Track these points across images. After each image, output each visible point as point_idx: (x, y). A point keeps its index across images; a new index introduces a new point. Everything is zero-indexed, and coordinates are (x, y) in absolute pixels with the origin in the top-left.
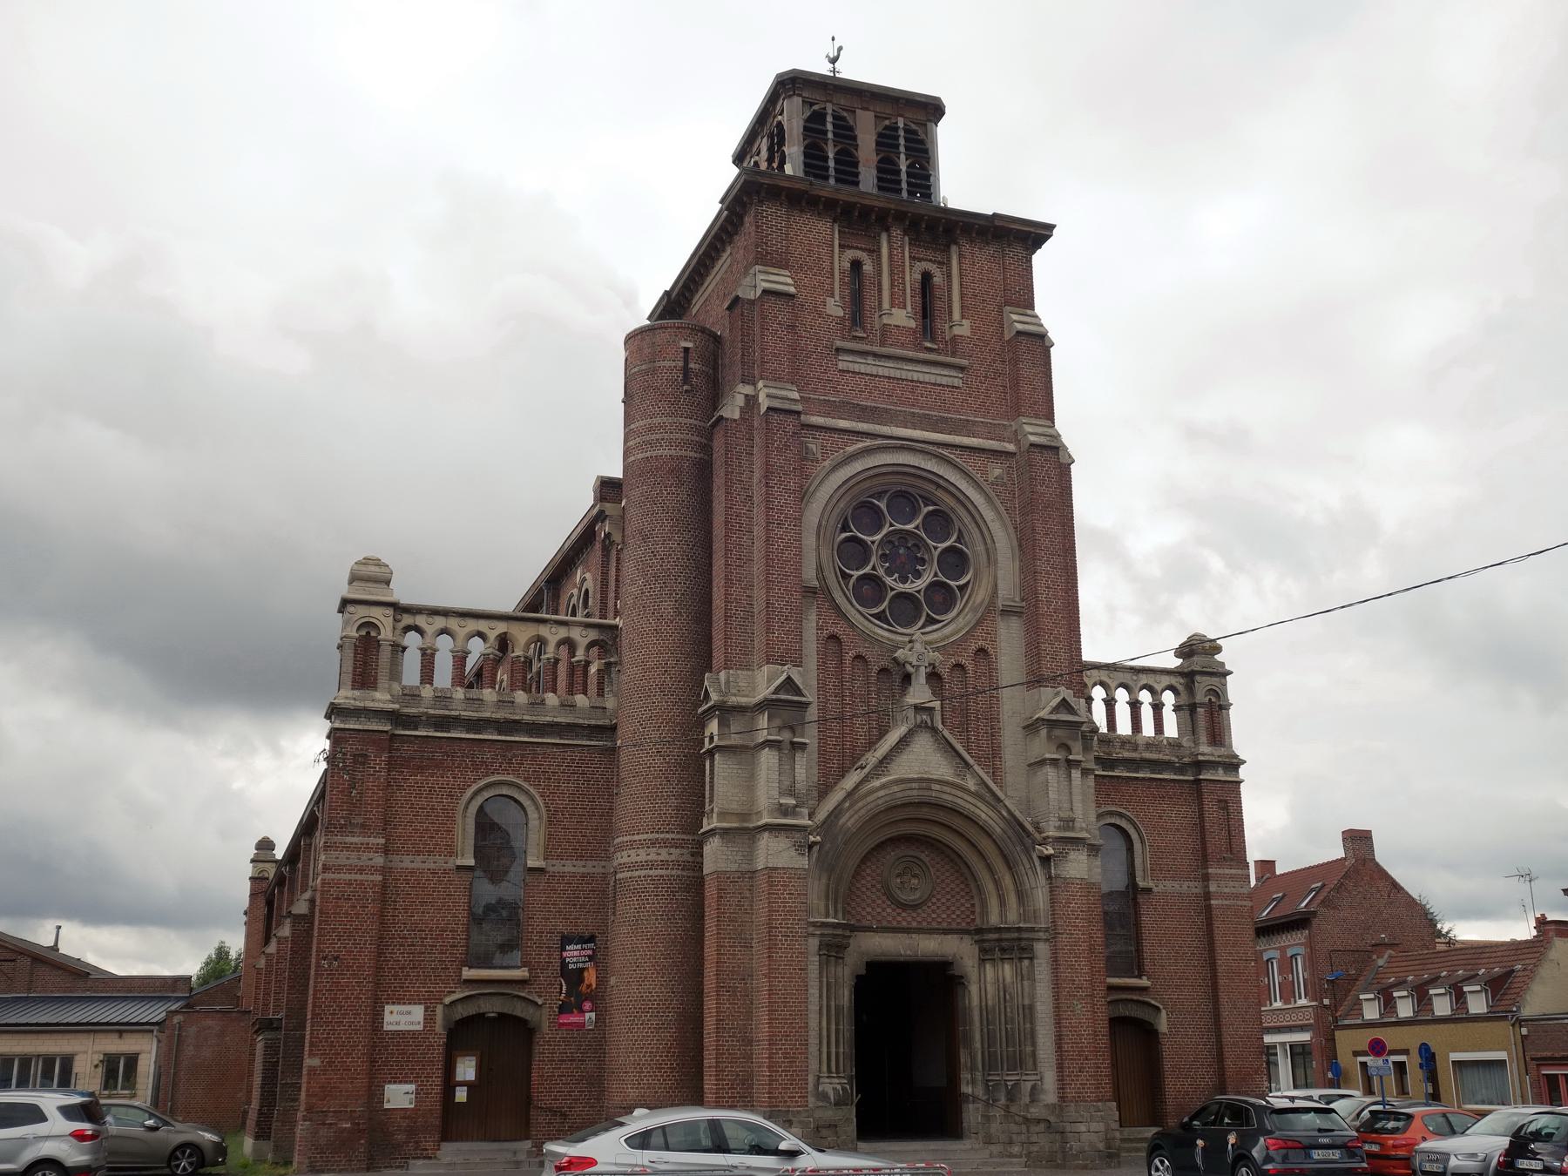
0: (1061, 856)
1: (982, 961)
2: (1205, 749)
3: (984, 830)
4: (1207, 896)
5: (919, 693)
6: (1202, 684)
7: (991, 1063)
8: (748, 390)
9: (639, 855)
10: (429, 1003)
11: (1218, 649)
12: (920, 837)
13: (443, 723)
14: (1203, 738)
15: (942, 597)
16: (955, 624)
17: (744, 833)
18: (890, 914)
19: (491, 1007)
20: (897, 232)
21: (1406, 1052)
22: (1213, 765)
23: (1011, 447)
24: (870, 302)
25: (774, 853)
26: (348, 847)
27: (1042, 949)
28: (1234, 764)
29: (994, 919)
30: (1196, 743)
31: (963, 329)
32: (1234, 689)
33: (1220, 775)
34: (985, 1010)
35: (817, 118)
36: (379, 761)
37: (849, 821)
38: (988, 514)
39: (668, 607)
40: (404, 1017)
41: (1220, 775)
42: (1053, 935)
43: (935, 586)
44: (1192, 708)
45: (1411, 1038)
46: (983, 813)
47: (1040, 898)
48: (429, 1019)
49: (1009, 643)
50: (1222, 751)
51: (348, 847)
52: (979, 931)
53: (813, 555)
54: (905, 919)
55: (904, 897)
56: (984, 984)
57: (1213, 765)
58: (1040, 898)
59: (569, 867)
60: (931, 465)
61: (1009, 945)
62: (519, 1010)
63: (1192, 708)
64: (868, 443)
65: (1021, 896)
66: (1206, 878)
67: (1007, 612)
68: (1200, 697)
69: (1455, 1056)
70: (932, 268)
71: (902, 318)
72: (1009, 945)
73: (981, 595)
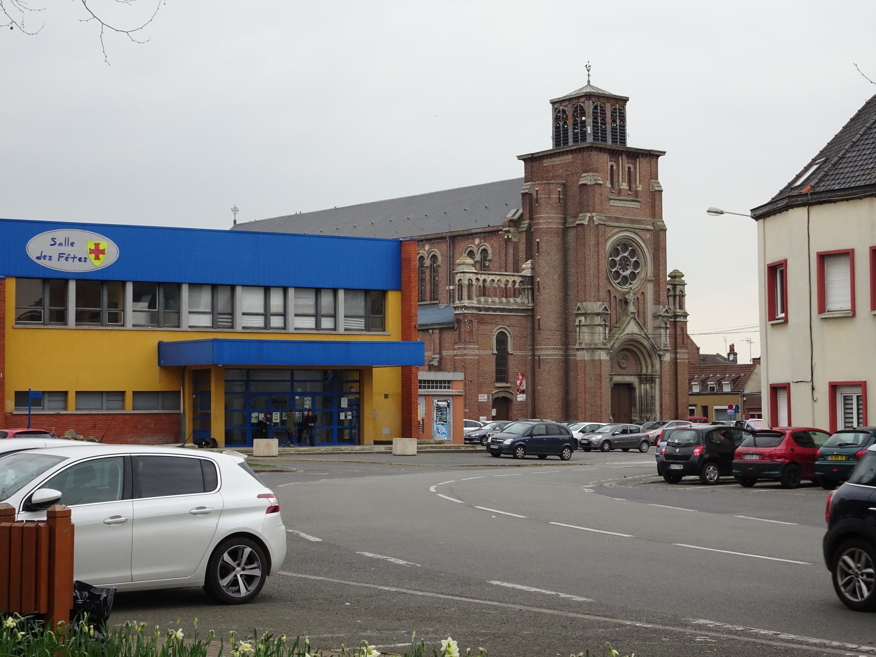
0: (664, 355)
1: (640, 384)
2: (678, 310)
3: (645, 347)
4: (676, 359)
5: (632, 308)
6: (679, 288)
7: (641, 411)
8: (589, 215)
9: (550, 351)
10: (488, 393)
11: (683, 276)
12: (631, 351)
13: (487, 309)
14: (678, 307)
15: (633, 276)
16: (636, 284)
17: (594, 349)
18: (619, 371)
19: (501, 395)
20: (624, 156)
21: (695, 405)
22: (680, 316)
23: (652, 228)
24: (615, 180)
25: (604, 356)
26: (471, 349)
27: (657, 380)
28: (685, 315)
29: (644, 372)
30: (675, 308)
31: (640, 189)
32: (687, 290)
33: (682, 319)
34: (641, 396)
35: (596, 108)
36: (475, 323)
37: (616, 346)
38: (646, 250)
39: (556, 277)
40: (483, 398)
41: (682, 319)
42: (661, 377)
43: (633, 273)
44: (675, 296)
45: (702, 401)
46: (645, 342)
47: (658, 366)
48: (488, 398)
49: (650, 289)
50: (682, 311)
51: (471, 349)
52: (640, 375)
53: (604, 264)
54: (623, 372)
55: (623, 366)
56: (641, 389)
57: (680, 316)
58: (658, 366)
59: (518, 353)
60: (632, 235)
61: (650, 379)
62: (509, 396)
63: (675, 296)
64: (617, 230)
65: (653, 366)
66: (676, 353)
67: (649, 281)
68: (678, 293)
69: (716, 407)
70: (630, 165)
71: (624, 186)
72: (650, 379)
73: (642, 275)
